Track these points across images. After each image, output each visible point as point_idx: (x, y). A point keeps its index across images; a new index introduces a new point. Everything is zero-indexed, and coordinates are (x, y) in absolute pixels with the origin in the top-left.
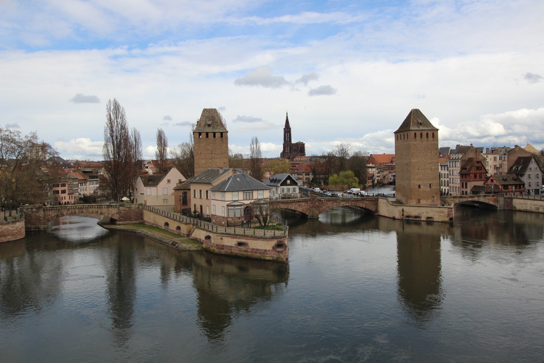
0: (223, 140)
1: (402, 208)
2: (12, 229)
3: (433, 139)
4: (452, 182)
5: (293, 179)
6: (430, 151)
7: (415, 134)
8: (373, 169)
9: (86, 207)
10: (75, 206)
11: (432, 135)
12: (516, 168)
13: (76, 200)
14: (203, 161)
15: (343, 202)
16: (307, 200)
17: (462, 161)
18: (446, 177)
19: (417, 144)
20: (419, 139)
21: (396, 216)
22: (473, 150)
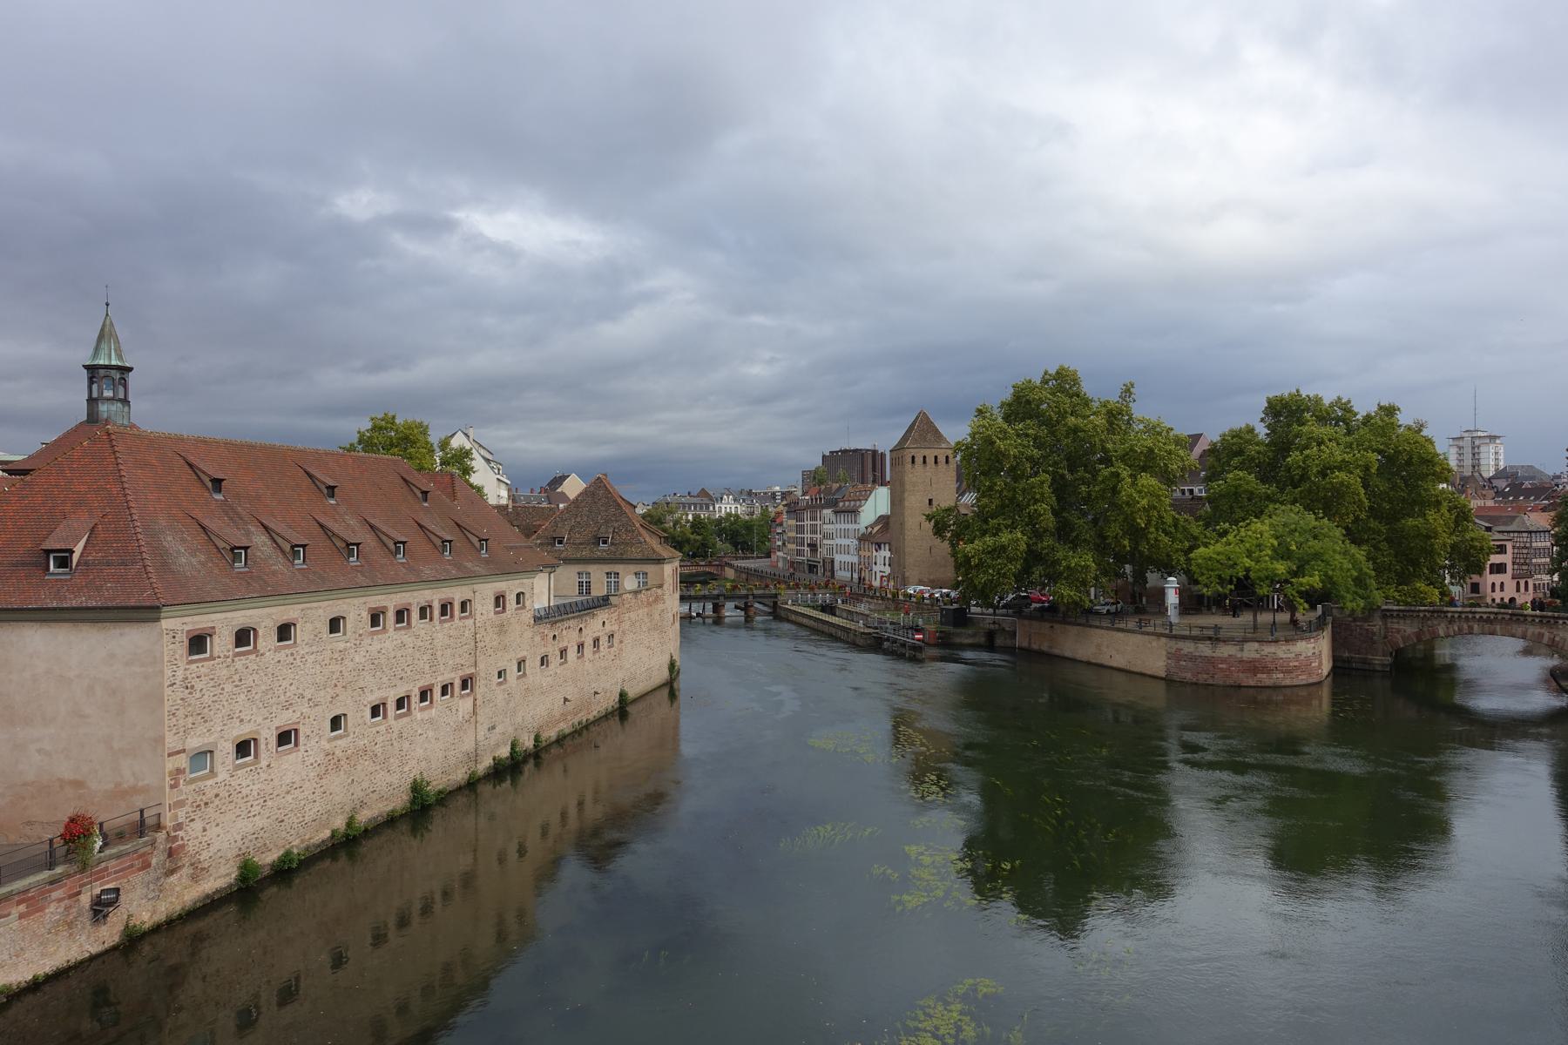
2: (1285, 656)
9: (1503, 618)
10: (1470, 612)
13: (1541, 595)
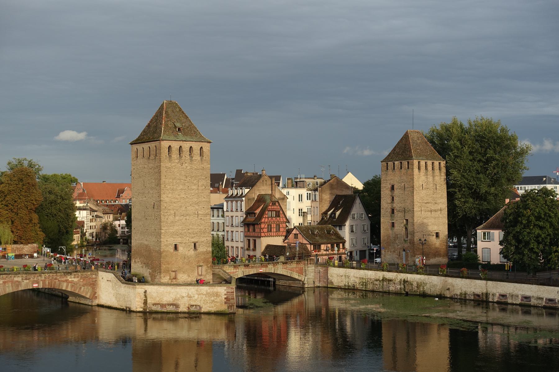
1: (144, 290)
4: (230, 239)
8: (81, 212)
12: (332, 213)
15: (28, 281)
17: (249, 199)
18: (221, 229)
20: (176, 158)
21: (132, 307)
22: (266, 181)
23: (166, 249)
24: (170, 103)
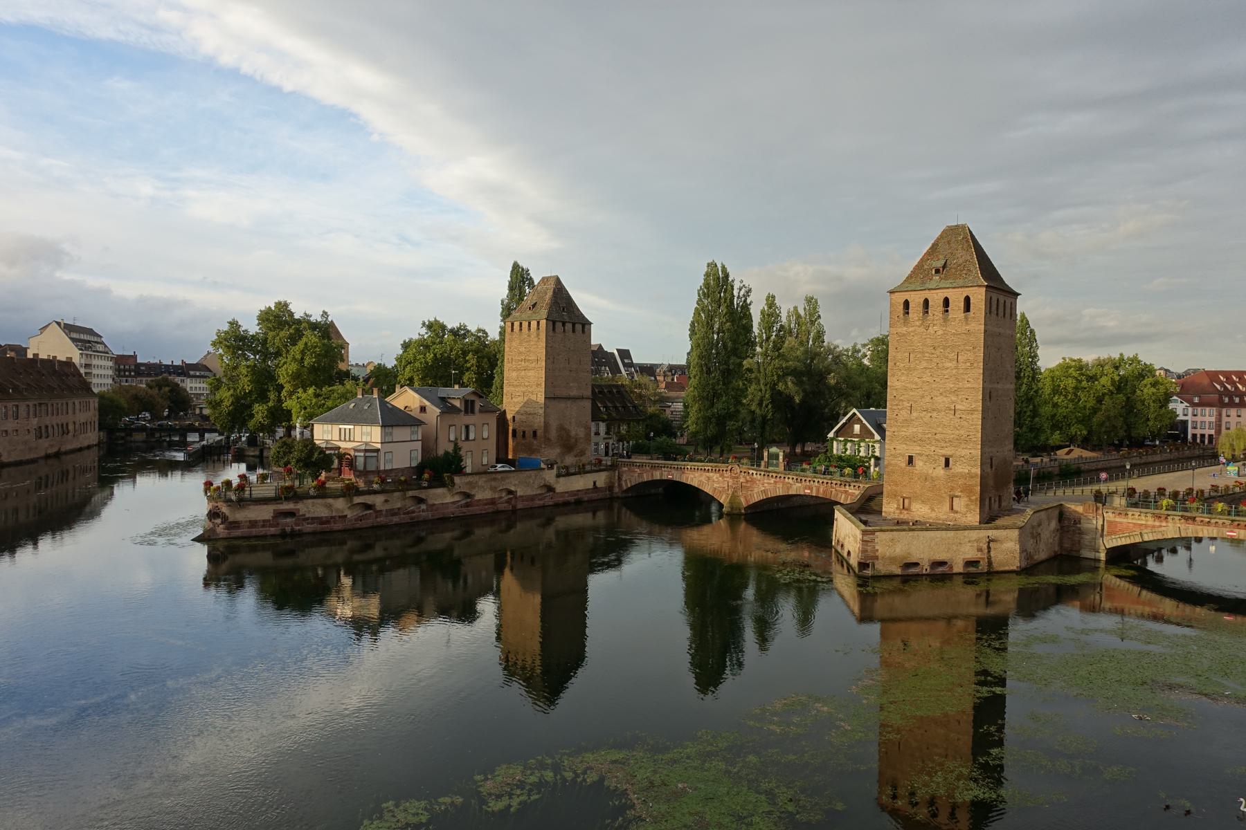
0: (538, 335)
3: (966, 318)
5: (864, 421)
6: (954, 357)
7: (907, 304)
11: (962, 305)
14: (514, 374)
15: (800, 485)
16: (721, 469)
19: (909, 333)
20: (917, 318)
23: (893, 462)
24: (952, 230)
